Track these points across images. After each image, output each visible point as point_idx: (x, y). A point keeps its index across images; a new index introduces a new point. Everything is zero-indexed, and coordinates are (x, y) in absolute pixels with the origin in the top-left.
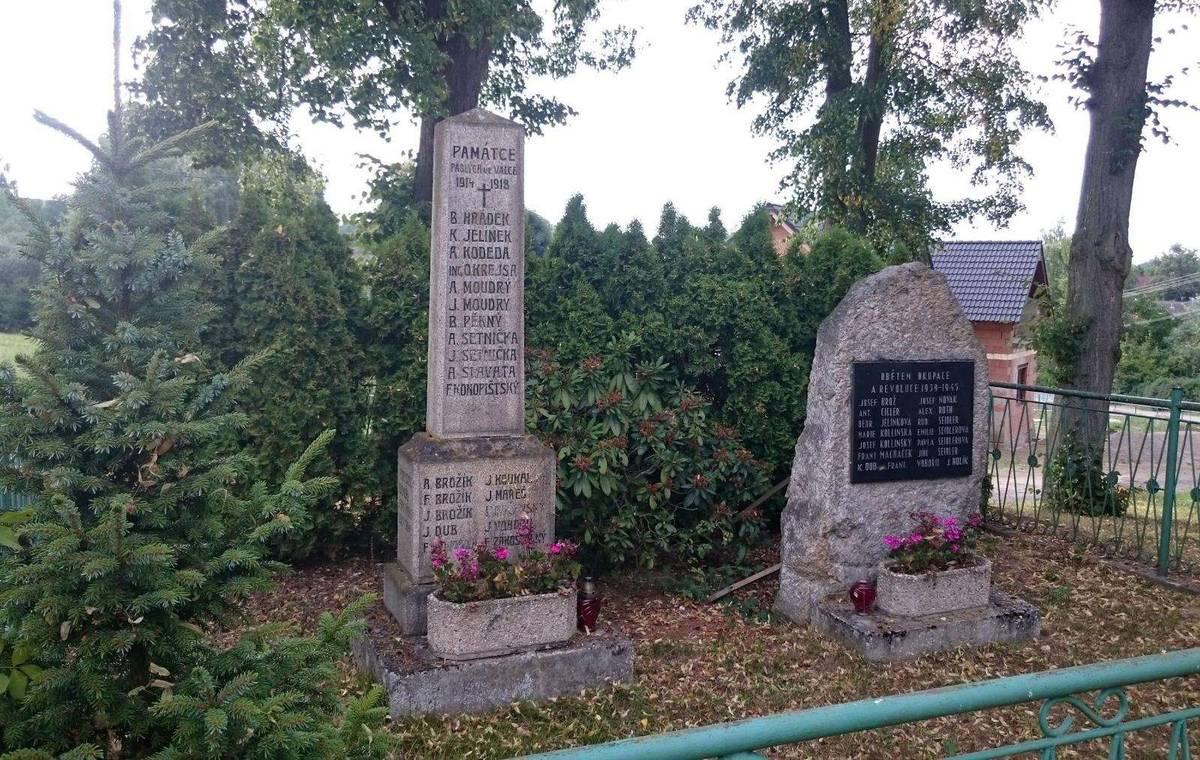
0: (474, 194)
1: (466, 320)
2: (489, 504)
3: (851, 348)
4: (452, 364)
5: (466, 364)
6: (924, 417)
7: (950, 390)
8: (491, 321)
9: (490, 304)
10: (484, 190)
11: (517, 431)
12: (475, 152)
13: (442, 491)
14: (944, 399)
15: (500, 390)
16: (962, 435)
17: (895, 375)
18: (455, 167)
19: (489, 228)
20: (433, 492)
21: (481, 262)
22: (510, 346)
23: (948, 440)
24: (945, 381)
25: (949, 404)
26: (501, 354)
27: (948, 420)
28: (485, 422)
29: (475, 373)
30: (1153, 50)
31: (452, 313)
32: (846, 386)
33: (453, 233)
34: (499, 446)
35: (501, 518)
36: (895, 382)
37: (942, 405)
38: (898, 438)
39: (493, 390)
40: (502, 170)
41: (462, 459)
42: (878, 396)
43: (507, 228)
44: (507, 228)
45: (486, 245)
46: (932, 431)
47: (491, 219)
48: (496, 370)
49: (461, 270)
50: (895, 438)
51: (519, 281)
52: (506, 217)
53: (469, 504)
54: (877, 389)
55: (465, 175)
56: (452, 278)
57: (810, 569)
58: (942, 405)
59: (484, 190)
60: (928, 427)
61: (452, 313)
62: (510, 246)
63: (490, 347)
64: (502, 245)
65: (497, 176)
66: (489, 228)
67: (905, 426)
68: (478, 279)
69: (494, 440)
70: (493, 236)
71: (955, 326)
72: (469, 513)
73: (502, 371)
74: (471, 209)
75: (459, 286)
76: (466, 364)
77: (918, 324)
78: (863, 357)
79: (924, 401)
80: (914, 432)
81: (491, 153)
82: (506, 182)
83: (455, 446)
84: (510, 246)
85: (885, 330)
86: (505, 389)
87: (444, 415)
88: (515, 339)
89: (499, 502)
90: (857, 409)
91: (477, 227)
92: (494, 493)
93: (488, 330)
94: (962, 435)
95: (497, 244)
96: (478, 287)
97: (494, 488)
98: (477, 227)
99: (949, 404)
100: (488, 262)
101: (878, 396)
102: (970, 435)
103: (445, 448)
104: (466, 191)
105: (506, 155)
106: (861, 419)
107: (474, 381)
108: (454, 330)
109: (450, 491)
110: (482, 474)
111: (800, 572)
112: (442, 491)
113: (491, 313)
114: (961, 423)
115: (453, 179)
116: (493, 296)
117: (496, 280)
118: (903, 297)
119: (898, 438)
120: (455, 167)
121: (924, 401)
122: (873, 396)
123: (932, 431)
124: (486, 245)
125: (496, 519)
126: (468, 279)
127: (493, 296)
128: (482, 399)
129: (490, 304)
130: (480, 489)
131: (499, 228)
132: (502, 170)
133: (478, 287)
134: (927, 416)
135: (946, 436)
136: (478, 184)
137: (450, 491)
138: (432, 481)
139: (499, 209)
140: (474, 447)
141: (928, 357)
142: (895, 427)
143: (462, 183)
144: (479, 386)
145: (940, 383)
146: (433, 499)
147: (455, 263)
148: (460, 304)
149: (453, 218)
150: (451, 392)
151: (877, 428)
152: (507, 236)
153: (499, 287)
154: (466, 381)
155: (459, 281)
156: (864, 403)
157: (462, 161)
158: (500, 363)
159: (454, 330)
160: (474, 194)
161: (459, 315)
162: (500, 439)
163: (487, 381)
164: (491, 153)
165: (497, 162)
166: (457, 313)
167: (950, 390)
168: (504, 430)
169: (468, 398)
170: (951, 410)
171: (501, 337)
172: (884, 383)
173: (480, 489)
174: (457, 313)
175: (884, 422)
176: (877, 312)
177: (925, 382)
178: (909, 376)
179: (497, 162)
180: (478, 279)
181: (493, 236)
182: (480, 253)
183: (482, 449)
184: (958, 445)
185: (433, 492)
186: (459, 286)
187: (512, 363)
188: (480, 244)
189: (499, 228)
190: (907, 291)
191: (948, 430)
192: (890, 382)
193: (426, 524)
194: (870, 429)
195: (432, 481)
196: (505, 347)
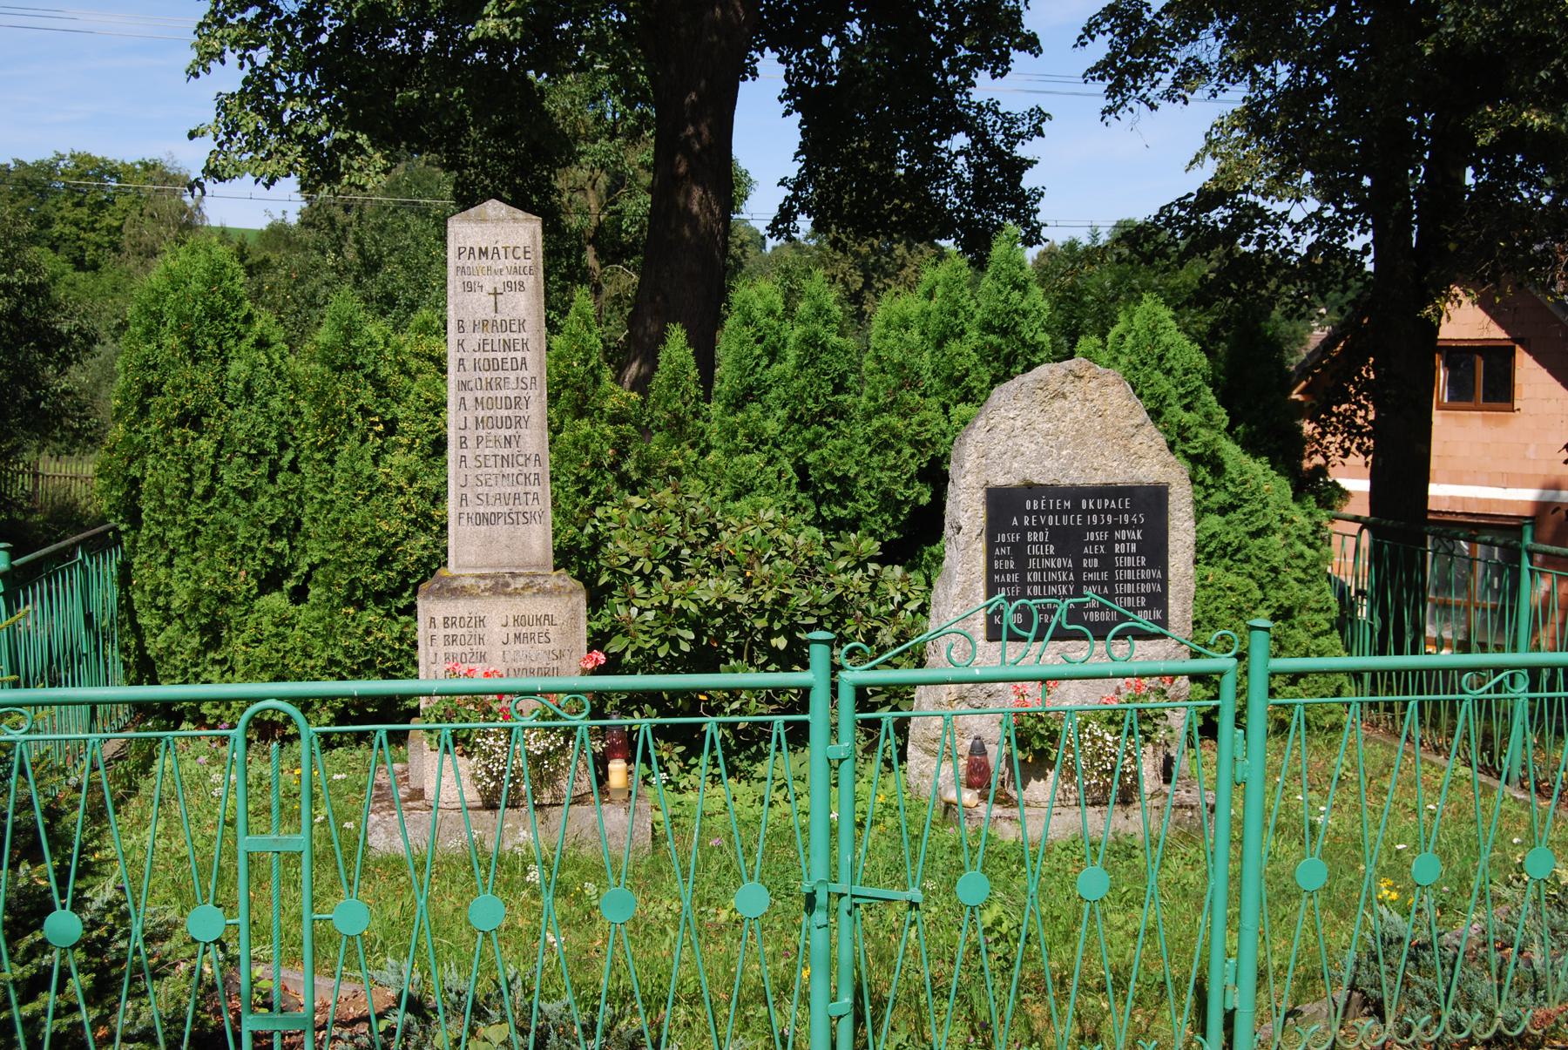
0: (484, 299)
1: (479, 440)
2: (506, 648)
3: (980, 469)
4: (464, 491)
5: (480, 490)
6: (1093, 556)
7: (1131, 522)
8: (508, 441)
9: (506, 422)
10: (496, 294)
11: (544, 566)
12: (483, 253)
13: (450, 631)
14: (1123, 534)
15: (522, 519)
16: (1152, 580)
17: (1047, 503)
18: (461, 270)
19: (503, 336)
20: (441, 632)
21: (495, 374)
22: (532, 469)
23: (1129, 588)
24: (1124, 511)
25: (1132, 541)
26: (521, 479)
27: (1129, 561)
28: (505, 556)
29: (491, 500)
30: (754, 74)
31: (462, 433)
32: (975, 515)
33: (460, 344)
34: (520, 583)
35: (521, 664)
36: (1047, 512)
37: (1120, 541)
38: (1054, 583)
39: (512, 519)
40: (516, 271)
41: (472, 596)
42: (1023, 530)
43: (524, 335)
44: (524, 335)
45: (500, 355)
46: (1105, 575)
47: (506, 326)
48: (516, 497)
49: (472, 385)
50: (1047, 584)
51: (540, 395)
52: (522, 324)
53: (482, 648)
54: (1021, 521)
55: (473, 279)
56: (462, 394)
57: (937, 747)
58: (1120, 541)
59: (496, 294)
60: (1099, 570)
61: (462, 433)
62: (528, 355)
63: (508, 470)
64: (519, 355)
65: (510, 278)
66: (503, 336)
67: (1063, 569)
68: (492, 394)
69: (513, 575)
70: (507, 345)
71: (1139, 439)
72: (483, 657)
73: (523, 498)
74: (481, 316)
75: (470, 402)
76: (480, 490)
77: (1080, 437)
78: (1001, 481)
79: (1091, 536)
80: (1078, 576)
81: (502, 252)
82: (521, 284)
83: (468, 582)
84: (528, 355)
85: (1033, 446)
86: (528, 518)
87: (466, 549)
88: (538, 459)
89: (518, 646)
90: (991, 546)
91: (490, 336)
92: (512, 636)
93: (506, 452)
94: (1152, 580)
95: (513, 354)
96: (492, 403)
97: (512, 630)
98: (490, 336)
99: (1132, 541)
100: (502, 374)
101: (1023, 530)
102: (1164, 582)
103: (455, 584)
104: (475, 296)
105: (520, 253)
106: (999, 558)
107: (490, 509)
108: (465, 452)
109: (459, 631)
110: (497, 613)
111: (926, 751)
112: (450, 631)
113: (508, 433)
114: (1149, 565)
115: (459, 284)
116: (510, 413)
117: (512, 394)
118: (1057, 404)
119: (1054, 583)
120: (461, 270)
121: (1091, 536)
122: (1015, 530)
123: (1105, 575)
124: (500, 355)
125: (515, 665)
126: (479, 394)
127: (510, 413)
128: (501, 529)
129: (506, 422)
130: (495, 631)
131: (515, 336)
132: (516, 271)
133: (492, 403)
134: (1099, 556)
135: (1127, 581)
136: (489, 288)
137: (459, 631)
138: (439, 620)
139: (514, 315)
140: (490, 583)
141: (1098, 479)
142: (1049, 569)
143: (469, 287)
144: (497, 516)
145: (1115, 513)
146: (440, 641)
147: (464, 377)
148: (471, 422)
149: (461, 327)
150: (464, 521)
151: (1022, 568)
152: (524, 345)
153: (517, 403)
154: (481, 510)
155: (469, 397)
156: (1002, 538)
157: (469, 263)
158: (520, 489)
159: (465, 452)
160: (484, 299)
161: (471, 435)
162: (521, 575)
163: (506, 509)
164: (502, 252)
165: (510, 262)
166: (467, 433)
167: (1131, 522)
168: (530, 565)
169: (483, 528)
170: (1134, 548)
171: (521, 460)
172: (1030, 513)
173: (495, 631)
174: (467, 433)
175: (1032, 563)
176: (1018, 423)
177: (1091, 512)
178: (1068, 504)
179: (510, 262)
180: (492, 394)
181: (507, 345)
182: (492, 365)
183: (499, 587)
184: (1145, 595)
185: (441, 632)
186: (470, 402)
187: (536, 489)
188: (491, 355)
189: (515, 336)
190: (1064, 396)
191: (1129, 574)
192: (1038, 512)
193: (434, 668)
194: (1011, 572)
195: (439, 620)
196: (525, 470)
